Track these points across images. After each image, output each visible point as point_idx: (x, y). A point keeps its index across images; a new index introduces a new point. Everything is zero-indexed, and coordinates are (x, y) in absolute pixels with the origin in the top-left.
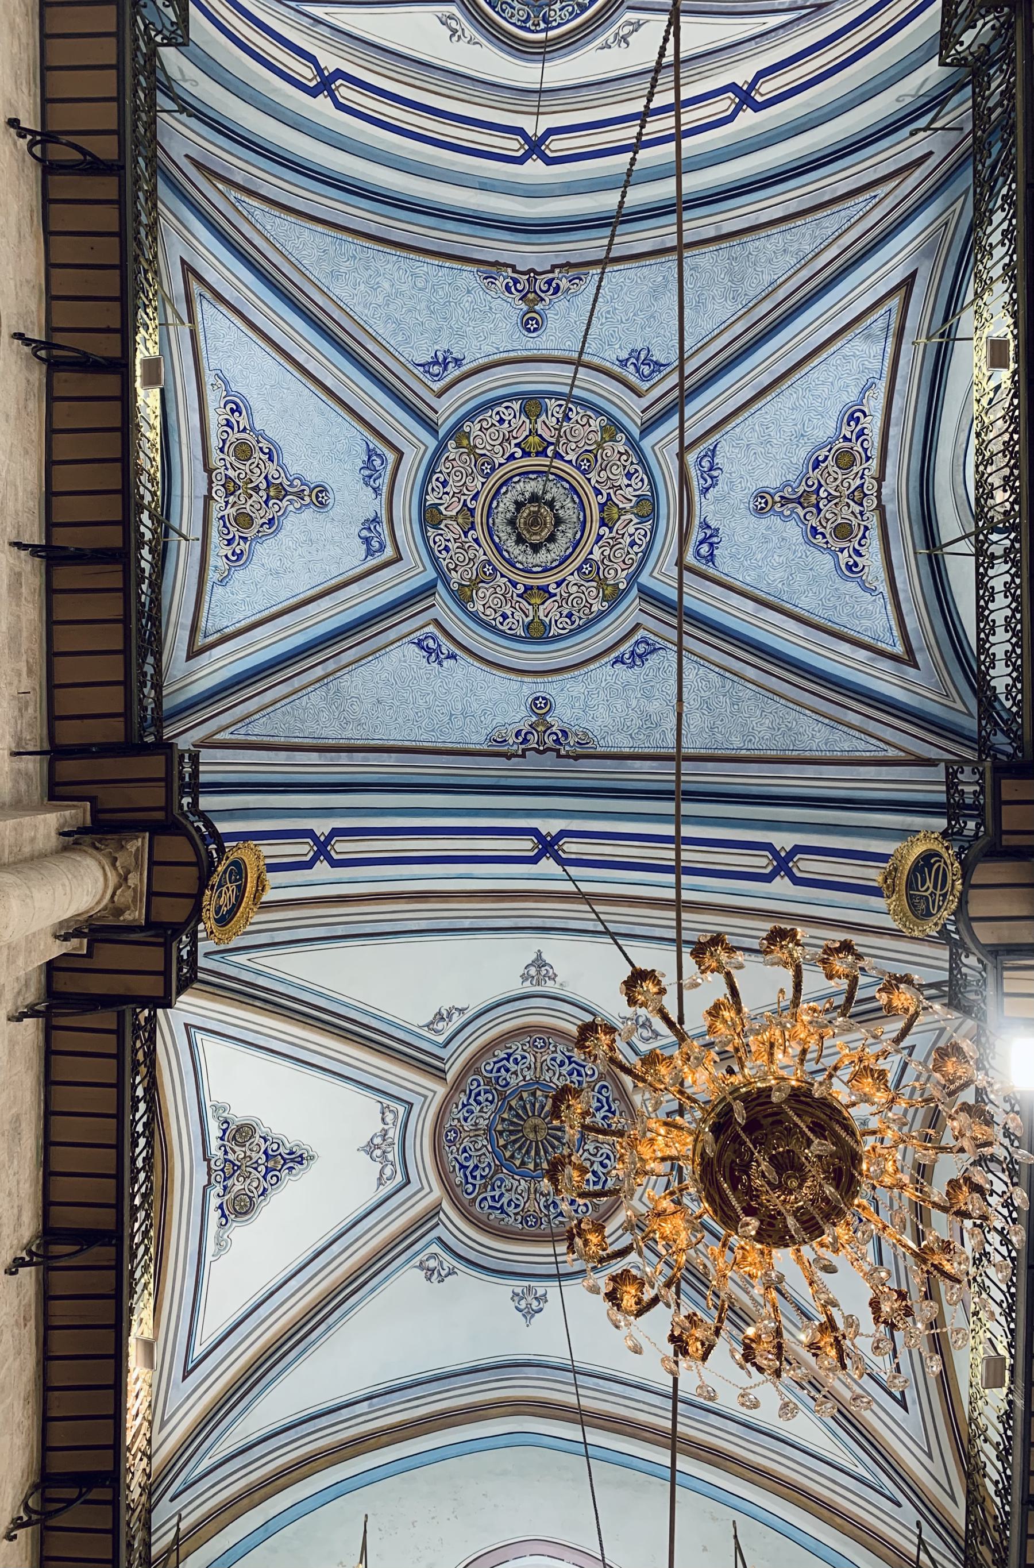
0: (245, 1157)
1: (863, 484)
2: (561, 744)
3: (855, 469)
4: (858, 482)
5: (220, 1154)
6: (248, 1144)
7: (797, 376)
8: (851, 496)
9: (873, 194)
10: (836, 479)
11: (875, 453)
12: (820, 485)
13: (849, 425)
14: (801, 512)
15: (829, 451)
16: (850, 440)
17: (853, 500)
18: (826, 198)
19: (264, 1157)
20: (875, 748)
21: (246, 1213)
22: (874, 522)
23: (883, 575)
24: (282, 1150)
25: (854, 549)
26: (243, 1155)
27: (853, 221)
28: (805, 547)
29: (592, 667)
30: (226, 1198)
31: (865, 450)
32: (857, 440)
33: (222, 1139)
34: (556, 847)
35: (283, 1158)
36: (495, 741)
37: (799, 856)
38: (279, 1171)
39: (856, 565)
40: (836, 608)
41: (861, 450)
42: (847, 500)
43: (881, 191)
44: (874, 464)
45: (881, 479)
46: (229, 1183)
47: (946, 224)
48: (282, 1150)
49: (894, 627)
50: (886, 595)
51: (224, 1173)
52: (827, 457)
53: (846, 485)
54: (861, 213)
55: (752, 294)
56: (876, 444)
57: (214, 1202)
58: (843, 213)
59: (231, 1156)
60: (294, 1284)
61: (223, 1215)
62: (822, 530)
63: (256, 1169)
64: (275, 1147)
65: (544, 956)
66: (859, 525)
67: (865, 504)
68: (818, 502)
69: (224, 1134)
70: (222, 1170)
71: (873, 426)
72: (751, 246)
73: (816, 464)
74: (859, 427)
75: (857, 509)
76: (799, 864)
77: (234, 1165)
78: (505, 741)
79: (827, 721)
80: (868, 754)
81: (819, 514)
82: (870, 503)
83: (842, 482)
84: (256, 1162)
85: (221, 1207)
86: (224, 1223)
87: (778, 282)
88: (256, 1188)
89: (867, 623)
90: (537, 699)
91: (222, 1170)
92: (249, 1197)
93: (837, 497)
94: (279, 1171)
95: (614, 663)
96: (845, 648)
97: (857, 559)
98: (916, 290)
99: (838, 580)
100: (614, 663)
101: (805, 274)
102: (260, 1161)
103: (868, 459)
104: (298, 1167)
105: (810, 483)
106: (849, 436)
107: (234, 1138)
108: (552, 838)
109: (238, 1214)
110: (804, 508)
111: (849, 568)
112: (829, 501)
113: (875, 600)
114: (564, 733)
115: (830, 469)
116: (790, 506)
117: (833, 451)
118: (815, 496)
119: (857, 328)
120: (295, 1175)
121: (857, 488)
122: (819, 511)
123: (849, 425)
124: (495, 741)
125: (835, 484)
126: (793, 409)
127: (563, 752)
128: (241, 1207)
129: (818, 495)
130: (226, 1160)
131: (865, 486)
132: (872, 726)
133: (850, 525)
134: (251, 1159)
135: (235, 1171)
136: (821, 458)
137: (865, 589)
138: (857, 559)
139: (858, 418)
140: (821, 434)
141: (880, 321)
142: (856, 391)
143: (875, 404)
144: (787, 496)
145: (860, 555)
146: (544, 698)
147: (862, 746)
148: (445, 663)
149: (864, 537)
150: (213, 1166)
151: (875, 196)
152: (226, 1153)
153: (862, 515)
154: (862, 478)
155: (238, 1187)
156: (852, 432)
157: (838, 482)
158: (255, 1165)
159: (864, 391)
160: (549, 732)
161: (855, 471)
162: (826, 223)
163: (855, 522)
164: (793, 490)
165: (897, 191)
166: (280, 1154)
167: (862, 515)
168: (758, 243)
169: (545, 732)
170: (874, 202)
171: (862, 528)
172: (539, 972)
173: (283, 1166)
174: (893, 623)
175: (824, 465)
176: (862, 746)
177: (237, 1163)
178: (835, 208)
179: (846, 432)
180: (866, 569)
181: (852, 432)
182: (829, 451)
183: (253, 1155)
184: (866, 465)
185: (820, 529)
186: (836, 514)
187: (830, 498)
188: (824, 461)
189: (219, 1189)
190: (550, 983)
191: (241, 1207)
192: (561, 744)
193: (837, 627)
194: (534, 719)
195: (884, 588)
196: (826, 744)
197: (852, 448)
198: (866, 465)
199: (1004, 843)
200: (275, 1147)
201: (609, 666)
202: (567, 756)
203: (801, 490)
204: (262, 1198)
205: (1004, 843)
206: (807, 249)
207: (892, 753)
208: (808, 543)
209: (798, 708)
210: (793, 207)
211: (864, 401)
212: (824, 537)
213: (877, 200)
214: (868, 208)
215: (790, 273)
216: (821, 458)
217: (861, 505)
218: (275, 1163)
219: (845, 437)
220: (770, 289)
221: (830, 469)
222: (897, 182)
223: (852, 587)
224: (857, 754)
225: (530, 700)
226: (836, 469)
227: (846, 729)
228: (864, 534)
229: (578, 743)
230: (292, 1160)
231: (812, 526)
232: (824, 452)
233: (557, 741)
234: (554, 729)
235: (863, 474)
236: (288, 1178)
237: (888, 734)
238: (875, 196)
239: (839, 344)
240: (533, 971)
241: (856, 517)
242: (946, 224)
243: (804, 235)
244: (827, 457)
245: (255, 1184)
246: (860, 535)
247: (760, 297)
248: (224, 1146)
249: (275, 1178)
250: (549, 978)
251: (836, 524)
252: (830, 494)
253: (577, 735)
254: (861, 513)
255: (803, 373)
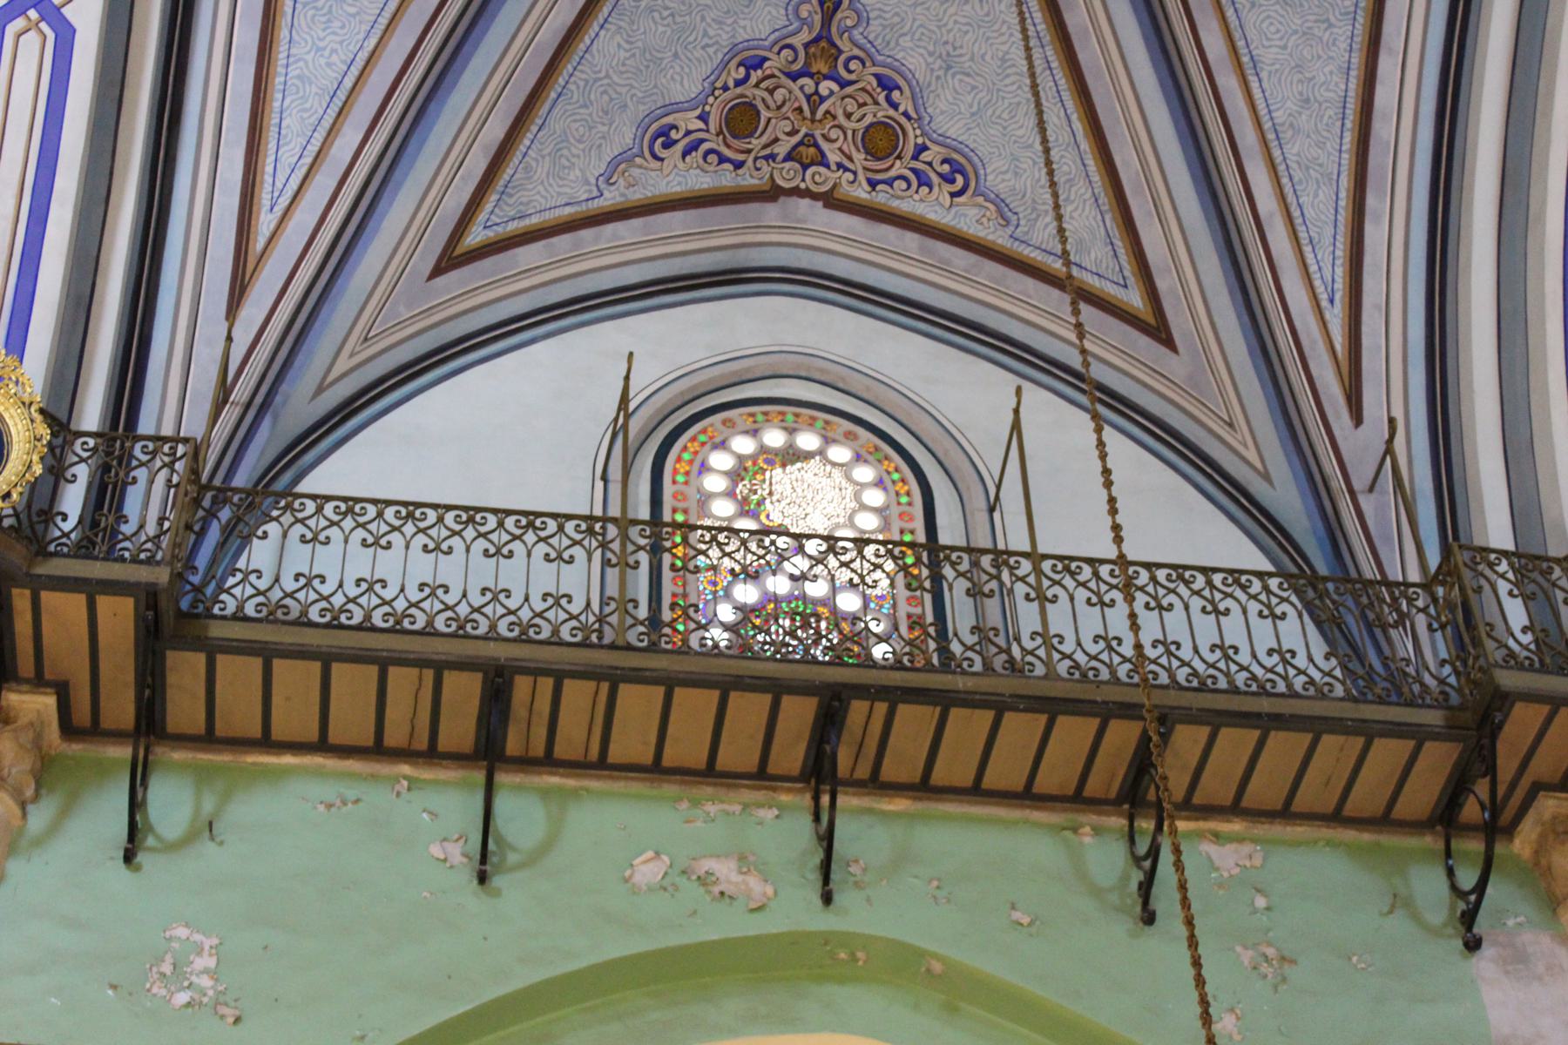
1: (828, 167)
3: (859, 157)
4: (833, 157)
7: (1062, 82)
8: (810, 141)
9: (1338, 297)
10: (848, 116)
11: (881, 197)
12: (843, 84)
13: (944, 161)
14: (798, 41)
15: (906, 114)
16: (915, 157)
17: (801, 143)
18: (1371, 201)
20: (279, 185)
22: (748, 179)
23: (637, 195)
25: (702, 141)
27: (1307, 249)
28: (725, 41)
31: (890, 183)
32: (914, 170)
37: (51, 36)
39: (668, 145)
40: (585, 106)
41: (893, 173)
42: (803, 131)
43: (1336, 318)
44: (861, 193)
45: (831, 200)
47: (1231, 425)
49: (527, 222)
50: (596, 204)
52: (895, 106)
53: (834, 134)
54: (1313, 268)
55: (1250, 18)
56: (895, 203)
58: (1329, 231)
62: (753, 79)
66: (749, 151)
67: (788, 165)
68: (811, 76)
71: (932, 206)
72: (1342, 31)
73: (887, 85)
74: (935, 179)
75: (781, 150)
76: (32, 34)
79: (348, 83)
80: (269, 169)
81: (788, 75)
82: (787, 175)
83: (840, 127)
87: (1252, 79)
89: (541, 171)
93: (813, 113)
96: (496, 130)
97: (680, 147)
98: (1144, 341)
99: (643, 109)
101: (1247, 138)
103: (873, 184)
105: (853, 65)
106: (925, 156)
110: (807, 46)
111: (664, 132)
112: (808, 98)
113: (587, 183)
115: (870, 108)
116: (818, 18)
117: (903, 120)
118: (825, 70)
119: (1114, 219)
121: (823, 154)
122: (794, 77)
123: (944, 161)
125: (840, 113)
126: (1003, 60)
129: (826, 77)
131: (822, 169)
132: (324, 183)
133: (751, 135)
136: (896, 94)
137: (614, 165)
138: (680, 147)
139: (952, 181)
140: (942, 106)
141: (1112, 263)
142: (1002, 188)
143: (968, 218)
144: (839, 15)
145: (684, 156)
147: (288, 155)
149: (723, 160)
151: (1332, 301)
153: (766, 158)
154: (840, 166)
156: (930, 164)
157: (842, 120)
159: (999, 203)
161: (855, 155)
162: (1326, 194)
163: (756, 143)
164: (848, 29)
165: (1321, 347)
167: (766, 158)
168: (1344, 45)
170: (1323, 298)
171: (741, 157)
174: (535, 220)
175: (881, 98)
176: (288, 155)
178: (1344, 216)
179: (933, 154)
180: (656, 164)
181: (930, 164)
182: (906, 114)
184: (861, 177)
185: (755, 76)
186: (779, 108)
187: (815, 99)
188: (888, 99)
193: (543, 111)
195: (612, 198)
196: (299, 77)
197: (899, 157)
198: (861, 177)
199: (15, 591)
203: (844, 44)
205: (15, 591)
206: (1292, 150)
207: (265, 222)
208: (734, 50)
209: (383, 21)
210: (1382, 129)
211: (980, 199)
212: (738, 83)
213: (1324, 303)
214: (1317, 283)
215: (1261, 105)
216: (896, 94)
217: (789, 157)
219: (925, 148)
220: (1245, 59)
221: (870, 108)
222: (1338, 348)
223: (624, 135)
224: (272, 146)
226: (869, 120)
227: (327, 124)
228: (729, 160)
231: (765, 59)
232: (906, 105)
235: (846, 169)
237: (305, 217)
238: (1332, 301)
239: (1096, 178)
241: (765, 147)
242: (1231, 425)
243: (1320, 145)
244: (895, 106)
246: (727, 152)
247: (1237, 35)
251: (761, 107)
252: (822, 99)
254: (771, 157)
255: (1066, 96)
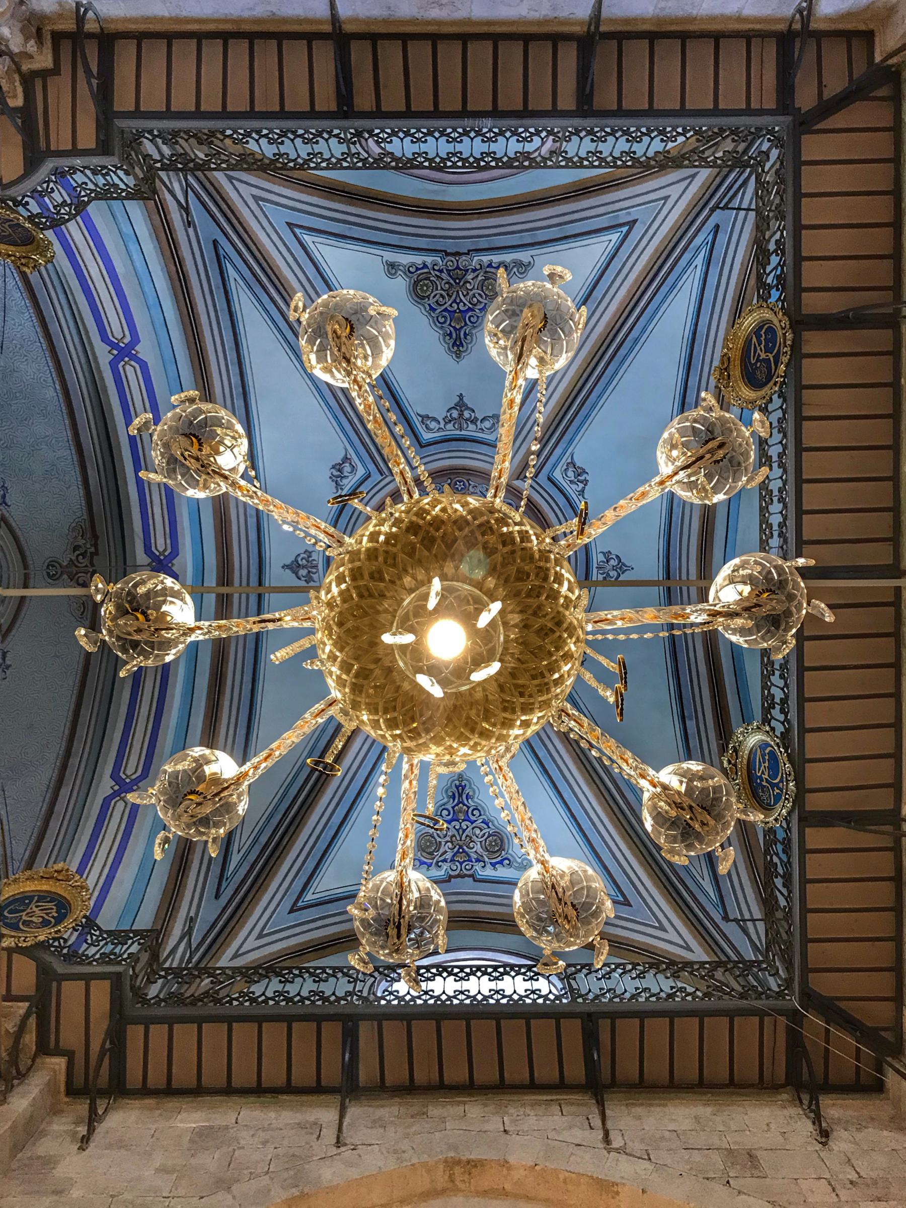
0: (452, 842)
2: (86, 551)
5: (445, 866)
6: (439, 839)
19: (453, 823)
21: (502, 841)
24: (449, 807)
26: (449, 844)
29: (14, 524)
30: (486, 859)
33: (430, 865)
34: (162, 557)
35: (457, 805)
36: (83, 612)
38: (468, 808)
46: (474, 856)
48: (449, 807)
51: (465, 861)
57: (489, 872)
59: (449, 856)
60: (567, 794)
61: (501, 862)
63: (464, 831)
64: (445, 813)
65: (288, 562)
69: (425, 863)
70: (461, 864)
77: (458, 852)
78: (83, 604)
84: (458, 830)
85: (493, 865)
86: (507, 862)
88: (481, 830)
90: (48, 574)
91: (461, 864)
92: (488, 837)
94: (468, 808)
95: (6, 505)
100: (6, 505)
102: (457, 827)
104: (467, 790)
107: (431, 853)
108: (153, 561)
109: (502, 849)
114: (76, 548)
120: (474, 792)
124: (83, 612)
127: (93, 550)
128: (496, 845)
130: (452, 860)
134: (454, 836)
135: (464, 851)
146: (48, 567)
148: (8, 662)
150: (456, 873)
152: (445, 861)
155: (478, 848)
158: (461, 832)
160: (76, 562)
166: (453, 808)
169: (76, 566)
172: (304, 567)
173: (464, 805)
177: (456, 849)
183: (450, 834)
189: (478, 867)
190: (314, 556)
191: (496, 845)
192: (86, 551)
194: (65, 576)
200: (445, 813)
201: (11, 509)
202: (96, 545)
204: (490, 824)
218: (460, 811)
225: (50, 581)
229: (82, 536)
230: (460, 795)
233: (84, 555)
234: (73, 558)
236: (476, 800)
240: (303, 572)
245: (477, 831)
248: (438, 862)
249: (475, 812)
250: (309, 557)
253: (76, 537)
